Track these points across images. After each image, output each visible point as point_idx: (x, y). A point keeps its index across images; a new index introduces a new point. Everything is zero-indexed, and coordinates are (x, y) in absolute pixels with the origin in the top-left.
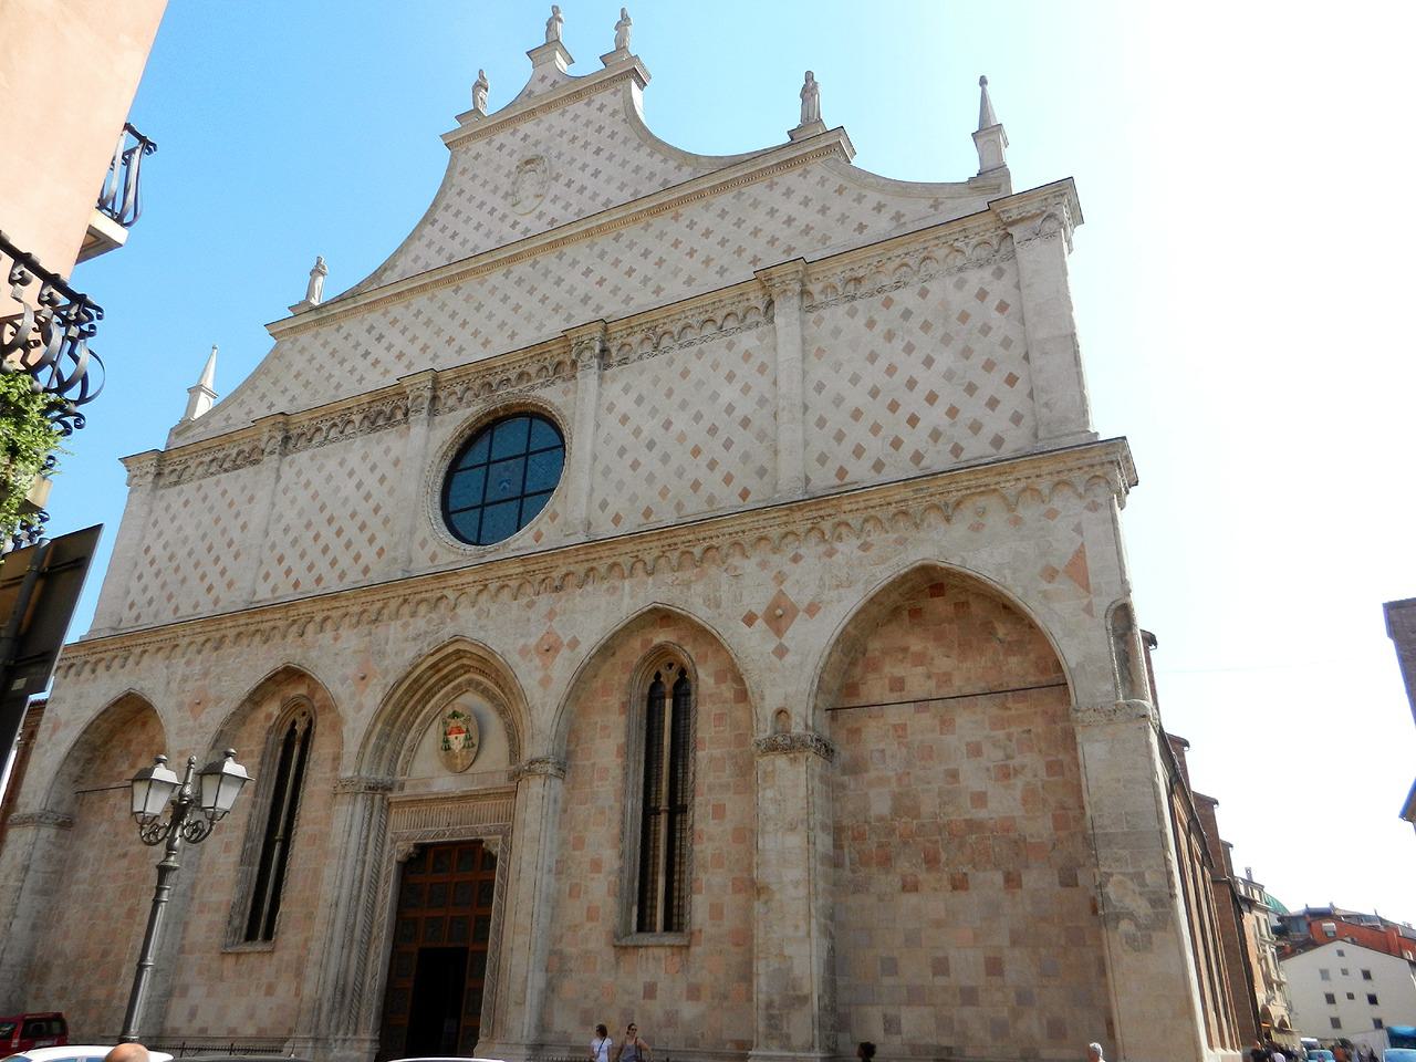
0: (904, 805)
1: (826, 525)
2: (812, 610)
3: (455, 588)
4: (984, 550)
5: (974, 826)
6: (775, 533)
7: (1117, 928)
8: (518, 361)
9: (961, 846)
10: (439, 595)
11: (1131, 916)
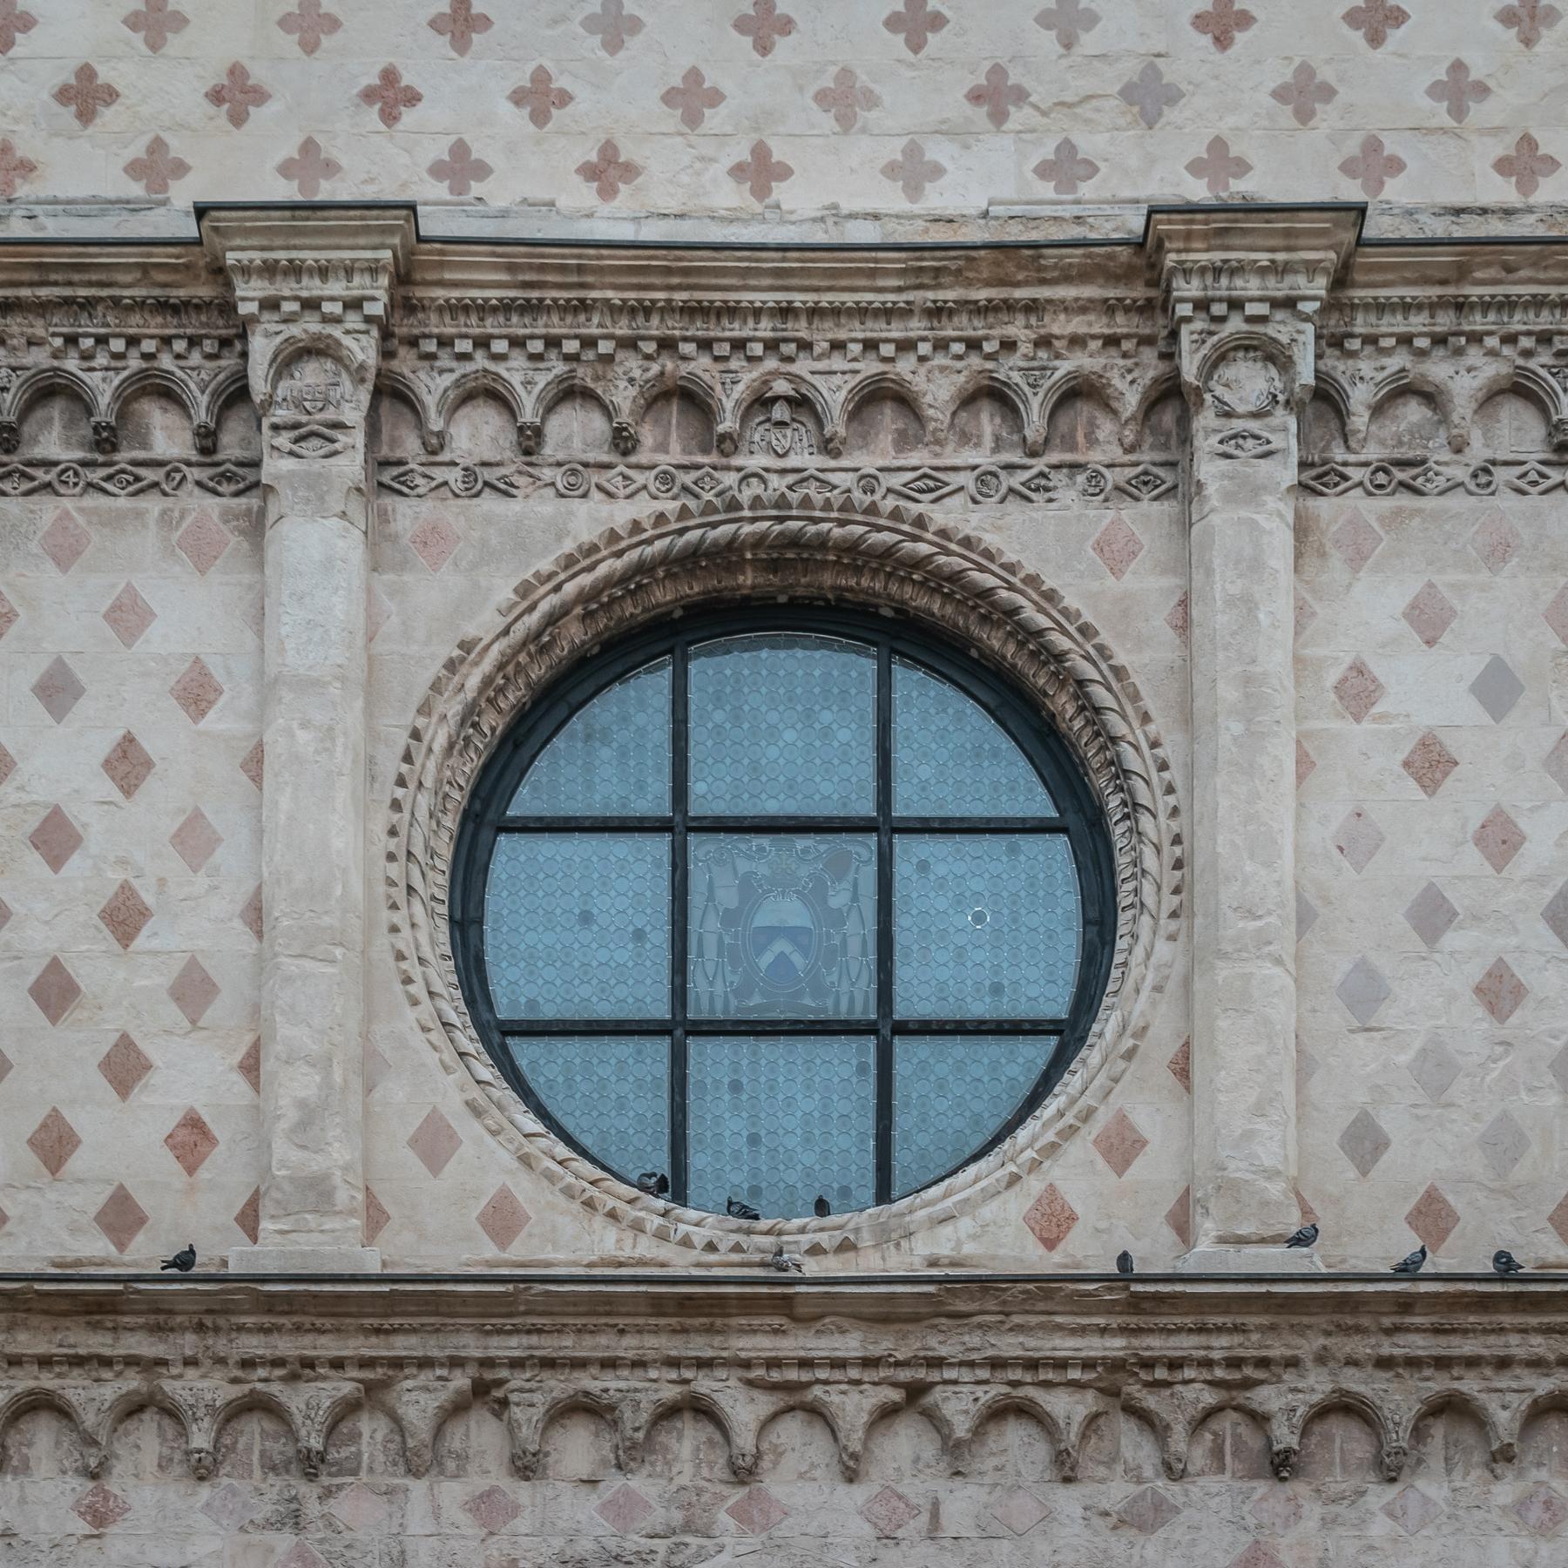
3: (759, 1375)
8: (862, 312)
10: (670, 1393)
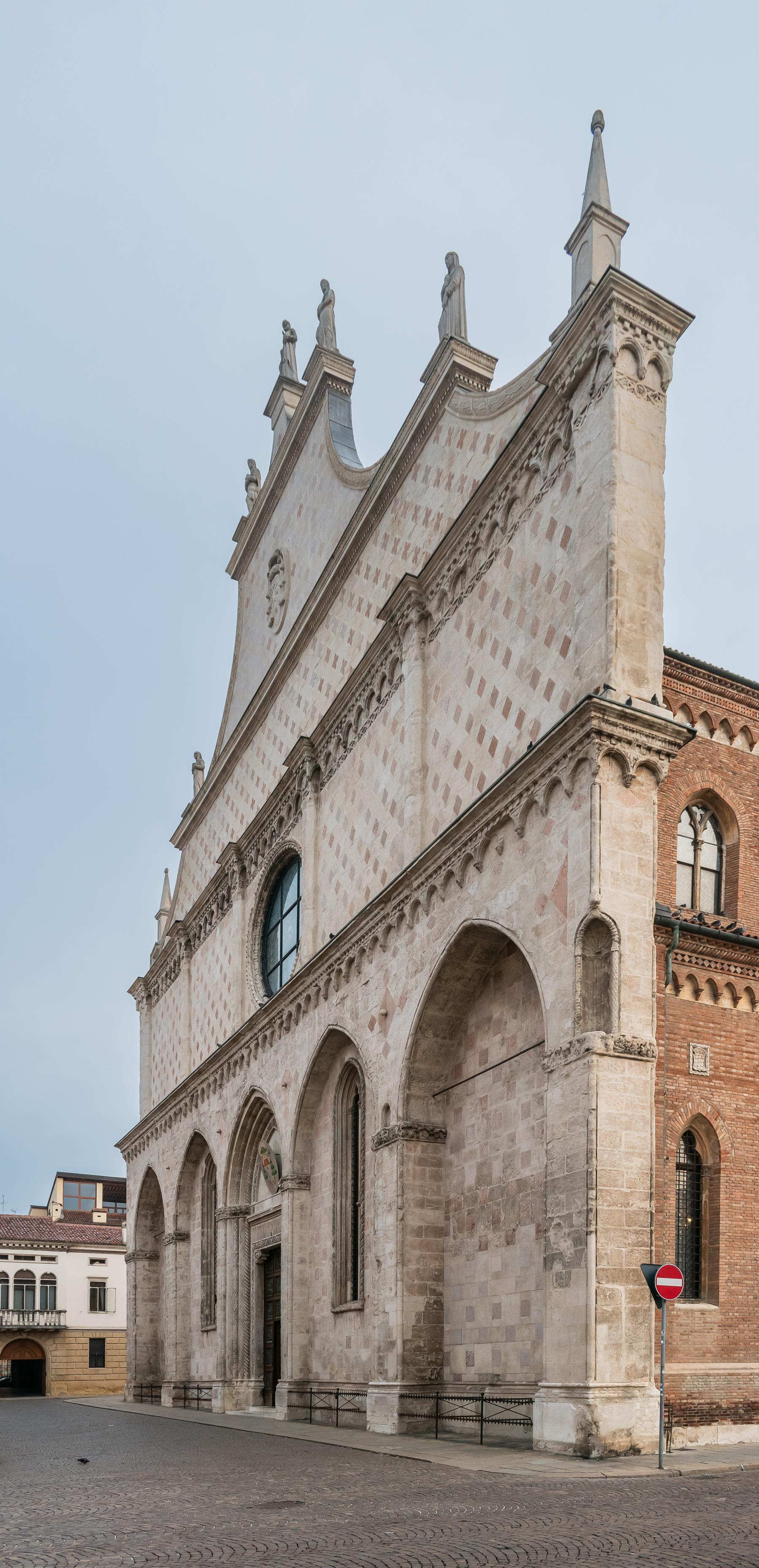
0: (482, 1179)
1: (407, 910)
2: (403, 1000)
4: (497, 895)
5: (522, 1184)
6: (379, 931)
7: (551, 1268)
9: (513, 1204)
11: (559, 1256)
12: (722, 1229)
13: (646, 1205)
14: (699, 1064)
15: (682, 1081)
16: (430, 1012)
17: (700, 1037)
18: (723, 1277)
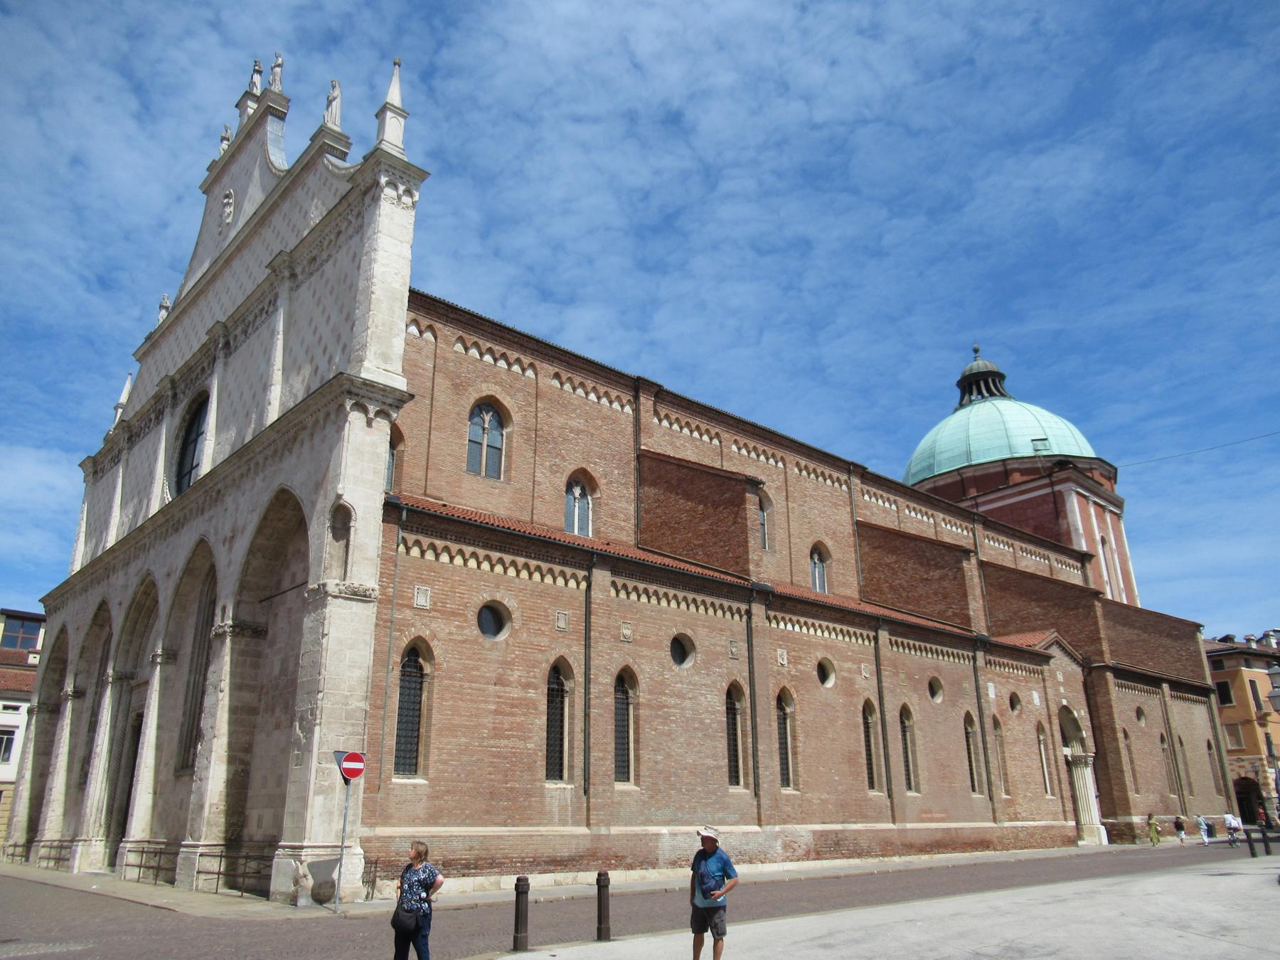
12: (434, 722)
13: (362, 705)
14: (422, 600)
15: (408, 613)
16: (259, 541)
17: (424, 582)
18: (433, 757)
